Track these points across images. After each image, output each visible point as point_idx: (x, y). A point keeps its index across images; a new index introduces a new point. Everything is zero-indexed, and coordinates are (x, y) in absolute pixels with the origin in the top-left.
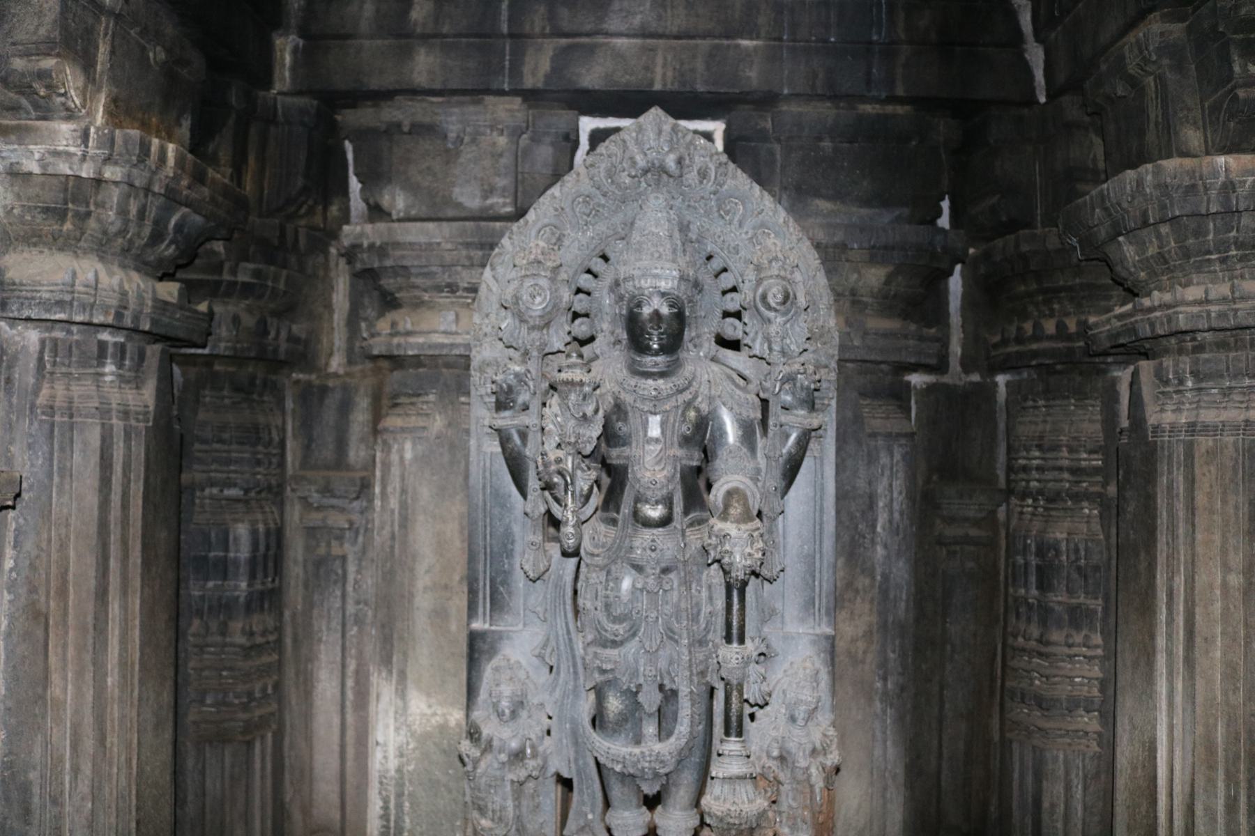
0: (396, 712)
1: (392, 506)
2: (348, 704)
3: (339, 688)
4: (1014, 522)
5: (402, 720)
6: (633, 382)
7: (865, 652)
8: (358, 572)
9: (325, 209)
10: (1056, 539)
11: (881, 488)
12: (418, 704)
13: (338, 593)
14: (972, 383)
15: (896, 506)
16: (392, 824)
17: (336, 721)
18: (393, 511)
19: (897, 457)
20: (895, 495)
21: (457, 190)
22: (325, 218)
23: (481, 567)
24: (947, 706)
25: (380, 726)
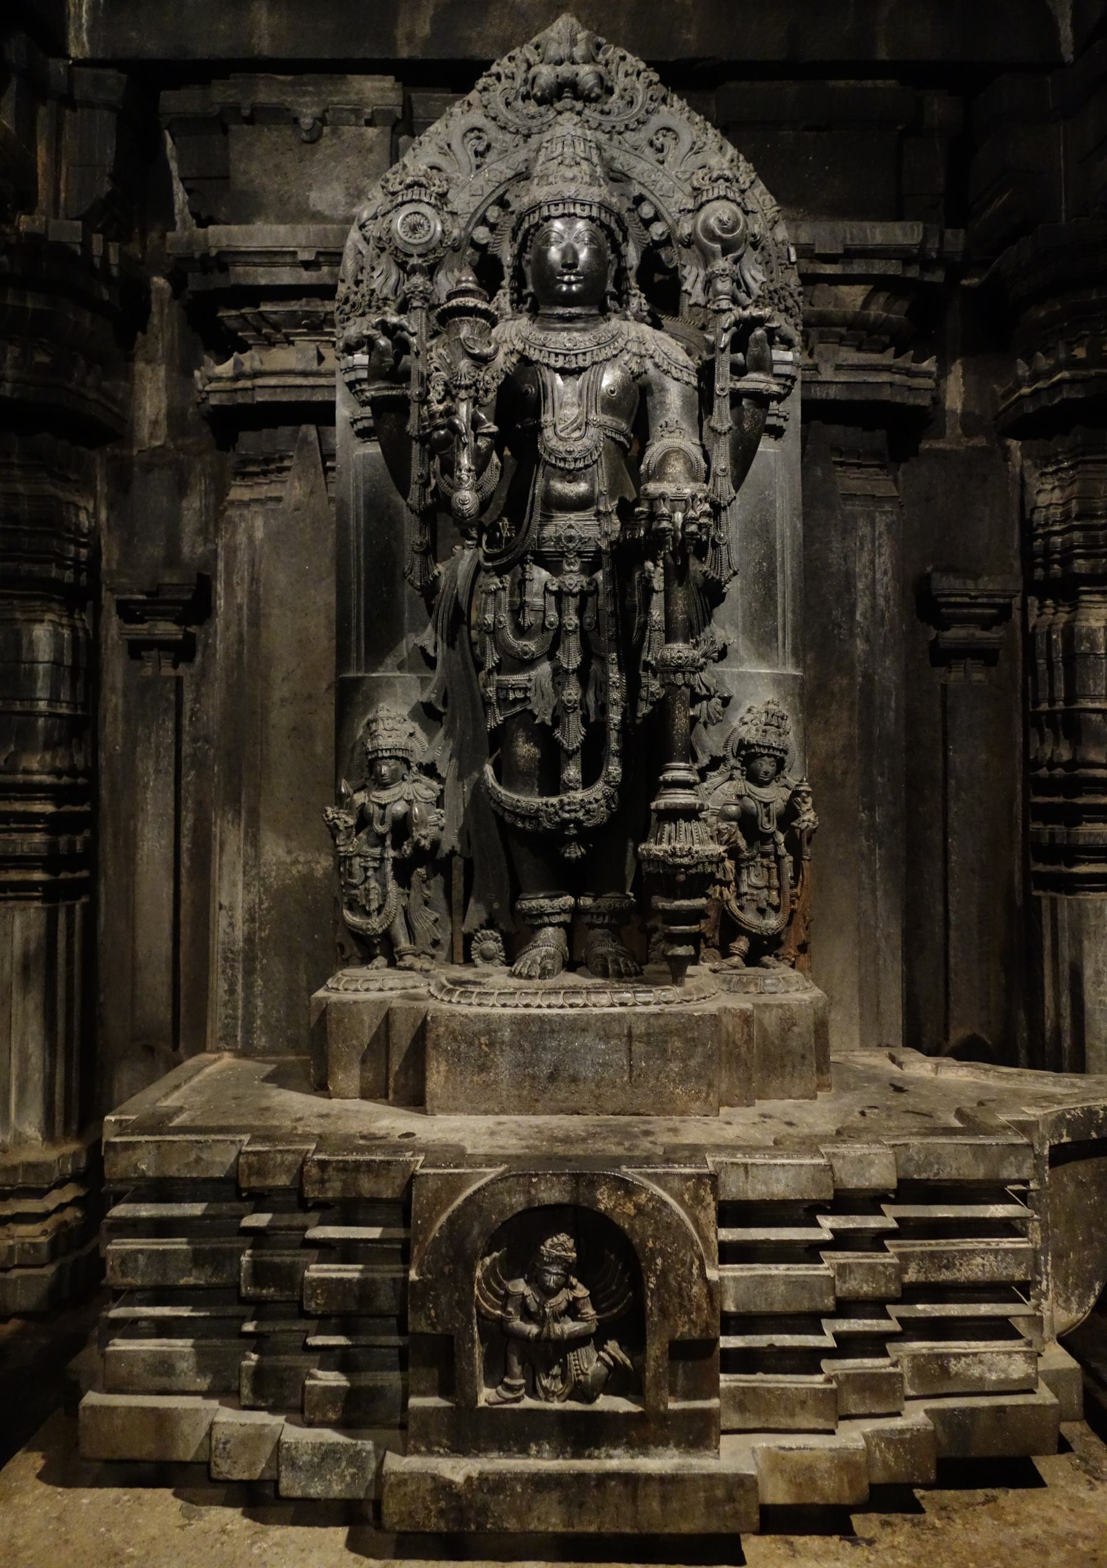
0: (246, 864)
1: (239, 600)
2: (183, 871)
3: (172, 849)
4: (1032, 621)
5: (253, 873)
6: (542, 336)
7: (845, 773)
8: (196, 700)
9: (144, 234)
10: (1090, 628)
11: (860, 566)
12: (274, 850)
13: (170, 725)
14: (974, 448)
15: (880, 590)
16: (240, 1012)
17: (167, 890)
18: (240, 607)
19: (881, 527)
20: (878, 576)
21: (313, 195)
22: (144, 248)
23: (353, 602)
24: (954, 858)
25: (225, 884)
